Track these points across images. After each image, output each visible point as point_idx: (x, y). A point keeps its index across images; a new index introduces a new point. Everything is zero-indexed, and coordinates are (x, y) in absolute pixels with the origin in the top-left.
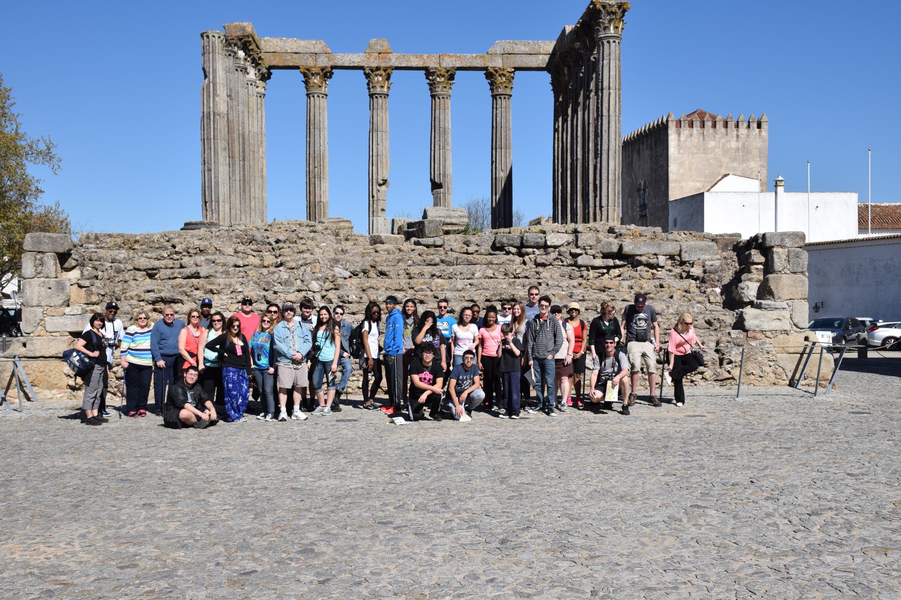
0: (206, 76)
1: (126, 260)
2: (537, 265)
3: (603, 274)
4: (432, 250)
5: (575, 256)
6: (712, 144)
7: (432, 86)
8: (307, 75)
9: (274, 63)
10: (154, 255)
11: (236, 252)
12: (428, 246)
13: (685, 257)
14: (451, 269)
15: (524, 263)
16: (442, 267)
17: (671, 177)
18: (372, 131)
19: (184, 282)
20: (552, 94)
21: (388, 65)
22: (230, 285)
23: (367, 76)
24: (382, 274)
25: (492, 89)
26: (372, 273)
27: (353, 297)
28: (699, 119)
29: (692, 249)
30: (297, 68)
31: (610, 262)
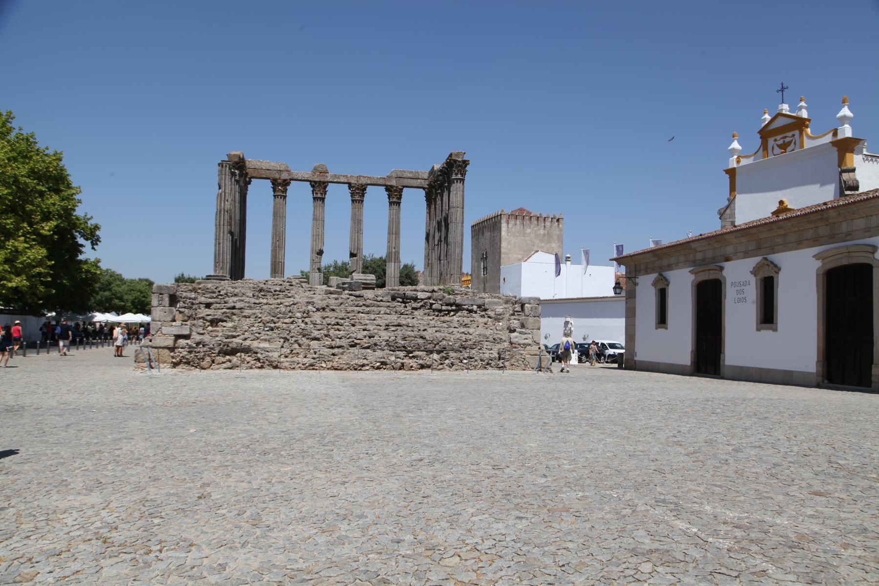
1: (195, 299)
2: (413, 308)
3: (446, 315)
5: (432, 304)
6: (529, 231)
10: (209, 296)
12: (357, 297)
13: (487, 306)
14: (368, 309)
15: (406, 307)
16: (364, 308)
17: (503, 250)
24: (333, 310)
26: (327, 310)
27: (318, 322)
28: (521, 215)
29: (490, 303)
31: (449, 308)
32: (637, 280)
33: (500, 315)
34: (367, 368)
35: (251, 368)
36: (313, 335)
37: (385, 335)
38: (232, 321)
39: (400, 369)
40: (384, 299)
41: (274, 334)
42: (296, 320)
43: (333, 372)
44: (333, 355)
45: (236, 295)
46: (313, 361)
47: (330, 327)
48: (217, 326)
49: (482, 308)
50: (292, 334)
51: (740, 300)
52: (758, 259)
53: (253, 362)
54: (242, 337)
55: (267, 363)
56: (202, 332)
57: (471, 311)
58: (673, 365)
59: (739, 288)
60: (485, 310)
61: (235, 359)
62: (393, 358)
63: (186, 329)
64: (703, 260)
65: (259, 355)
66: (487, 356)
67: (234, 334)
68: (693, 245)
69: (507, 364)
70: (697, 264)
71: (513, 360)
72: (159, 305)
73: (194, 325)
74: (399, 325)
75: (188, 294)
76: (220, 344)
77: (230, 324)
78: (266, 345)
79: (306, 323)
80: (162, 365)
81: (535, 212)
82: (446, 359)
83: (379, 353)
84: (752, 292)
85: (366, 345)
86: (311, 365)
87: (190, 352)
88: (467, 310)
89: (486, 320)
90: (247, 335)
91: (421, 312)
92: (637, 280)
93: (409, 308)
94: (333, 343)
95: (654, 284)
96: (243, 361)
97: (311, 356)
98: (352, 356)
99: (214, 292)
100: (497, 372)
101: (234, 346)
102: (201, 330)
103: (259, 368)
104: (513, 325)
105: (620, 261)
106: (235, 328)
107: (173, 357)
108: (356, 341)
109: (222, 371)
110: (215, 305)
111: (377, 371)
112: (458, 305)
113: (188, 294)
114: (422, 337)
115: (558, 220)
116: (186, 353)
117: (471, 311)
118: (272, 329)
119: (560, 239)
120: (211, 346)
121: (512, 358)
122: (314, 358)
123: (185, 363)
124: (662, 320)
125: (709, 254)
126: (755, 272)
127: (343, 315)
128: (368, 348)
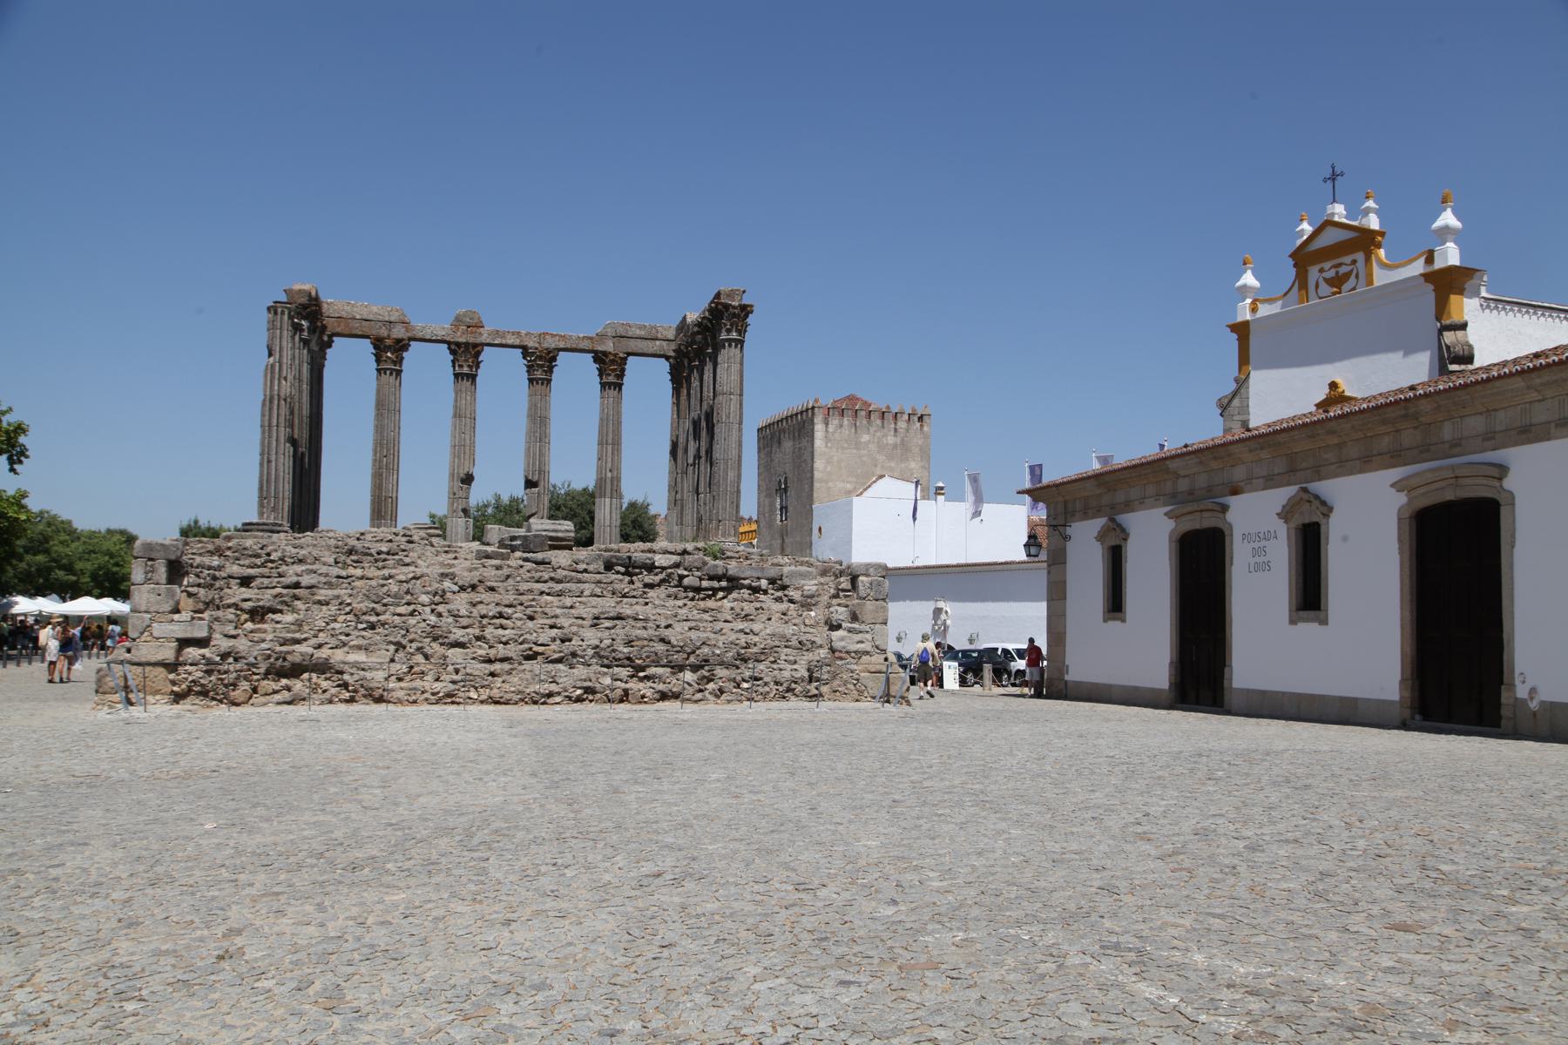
0: (270, 355)
1: (219, 568)
3: (709, 597)
4: (541, 567)
5: (682, 577)
6: (865, 438)
7: (530, 369)
8: (379, 345)
9: (338, 330)
10: (247, 562)
11: (336, 563)
12: (537, 563)
13: (786, 581)
14: (560, 587)
15: (632, 582)
16: (550, 584)
17: (817, 475)
18: (455, 416)
19: (285, 591)
20: (668, 387)
21: (479, 340)
22: (338, 597)
23: (453, 352)
24: (492, 589)
25: (601, 375)
26: (480, 589)
27: (463, 612)
28: (851, 409)
30: (367, 337)
31: (715, 584)
32: (1069, 531)
33: (812, 596)
34: (558, 699)
35: (331, 702)
36: (452, 638)
37: (592, 636)
38: (295, 610)
39: (621, 701)
40: (591, 568)
41: (376, 637)
42: (419, 608)
43: (492, 707)
44: (492, 674)
45: (300, 561)
46: (452, 687)
47: (485, 621)
48: (262, 621)
49: (778, 583)
50: (411, 636)
51: (1259, 567)
52: (1291, 490)
53: (333, 691)
54: (313, 641)
55: (362, 691)
56: (233, 632)
57: (756, 590)
58: (1136, 689)
59: (1256, 545)
60: (784, 588)
61: (298, 685)
62: (607, 681)
63: (201, 627)
64: (1191, 493)
65: (346, 677)
66: (787, 674)
67: (297, 635)
68: (1171, 465)
69: (824, 689)
70: (1179, 501)
71: (836, 683)
72: (147, 581)
73: (217, 619)
74: (619, 617)
75: (206, 560)
76: (269, 657)
77: (289, 618)
78: (360, 657)
79: (440, 615)
80: (150, 699)
81: (878, 403)
82: (710, 680)
83: (580, 671)
84: (1282, 552)
85: (556, 656)
86: (449, 695)
87: (209, 672)
88: (749, 587)
89: (784, 606)
90: (322, 637)
91: (661, 592)
92: (1069, 531)
93: (638, 584)
94: (492, 652)
95: (1101, 537)
96: (314, 691)
97: (448, 678)
98: (529, 676)
99: (257, 556)
100: (807, 704)
101: (297, 659)
102: (230, 629)
103: (347, 701)
104: (835, 617)
105: (1037, 494)
106: (299, 624)
107: (174, 683)
108: (536, 648)
109: (271, 708)
110: (259, 581)
111: (577, 706)
112: (731, 579)
113: (206, 560)
114: (663, 640)
115: (921, 418)
116: (200, 674)
117: (756, 590)
118: (372, 627)
119: (925, 454)
120: (252, 660)
121: (834, 678)
122: (454, 682)
123: (199, 694)
124: (1115, 605)
125: (1202, 481)
126: (1286, 514)
127: (511, 598)
128: (559, 661)
